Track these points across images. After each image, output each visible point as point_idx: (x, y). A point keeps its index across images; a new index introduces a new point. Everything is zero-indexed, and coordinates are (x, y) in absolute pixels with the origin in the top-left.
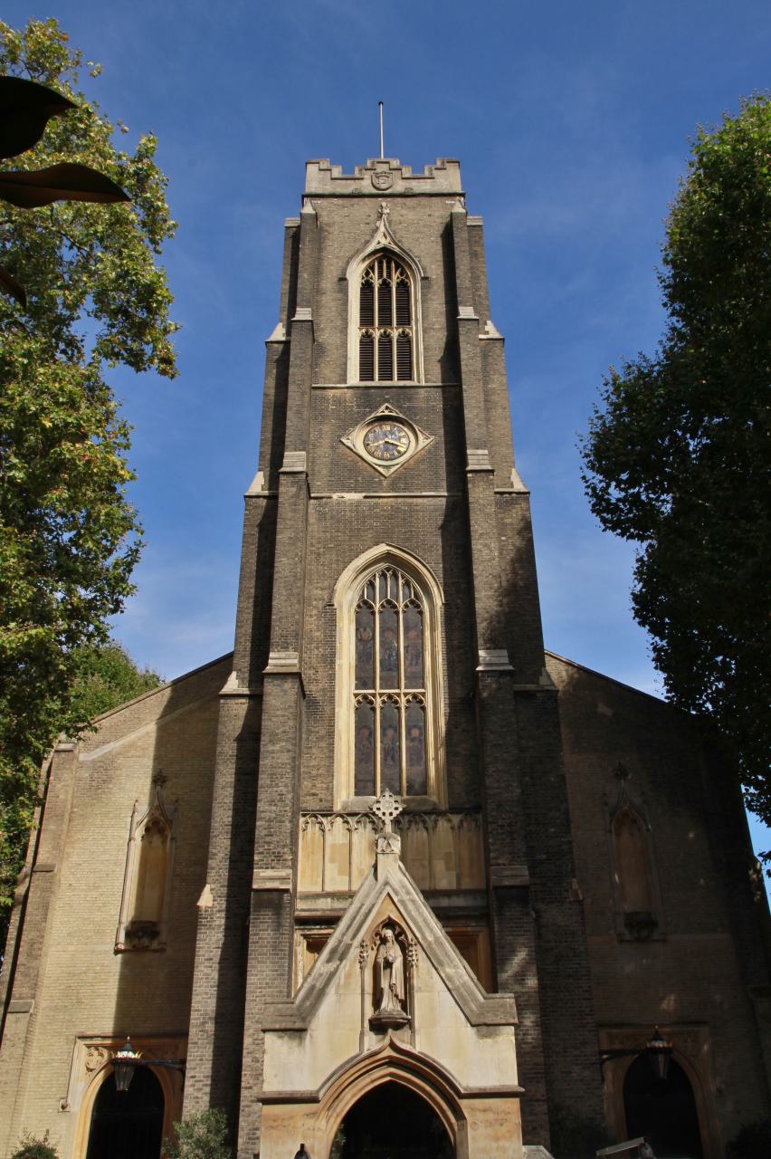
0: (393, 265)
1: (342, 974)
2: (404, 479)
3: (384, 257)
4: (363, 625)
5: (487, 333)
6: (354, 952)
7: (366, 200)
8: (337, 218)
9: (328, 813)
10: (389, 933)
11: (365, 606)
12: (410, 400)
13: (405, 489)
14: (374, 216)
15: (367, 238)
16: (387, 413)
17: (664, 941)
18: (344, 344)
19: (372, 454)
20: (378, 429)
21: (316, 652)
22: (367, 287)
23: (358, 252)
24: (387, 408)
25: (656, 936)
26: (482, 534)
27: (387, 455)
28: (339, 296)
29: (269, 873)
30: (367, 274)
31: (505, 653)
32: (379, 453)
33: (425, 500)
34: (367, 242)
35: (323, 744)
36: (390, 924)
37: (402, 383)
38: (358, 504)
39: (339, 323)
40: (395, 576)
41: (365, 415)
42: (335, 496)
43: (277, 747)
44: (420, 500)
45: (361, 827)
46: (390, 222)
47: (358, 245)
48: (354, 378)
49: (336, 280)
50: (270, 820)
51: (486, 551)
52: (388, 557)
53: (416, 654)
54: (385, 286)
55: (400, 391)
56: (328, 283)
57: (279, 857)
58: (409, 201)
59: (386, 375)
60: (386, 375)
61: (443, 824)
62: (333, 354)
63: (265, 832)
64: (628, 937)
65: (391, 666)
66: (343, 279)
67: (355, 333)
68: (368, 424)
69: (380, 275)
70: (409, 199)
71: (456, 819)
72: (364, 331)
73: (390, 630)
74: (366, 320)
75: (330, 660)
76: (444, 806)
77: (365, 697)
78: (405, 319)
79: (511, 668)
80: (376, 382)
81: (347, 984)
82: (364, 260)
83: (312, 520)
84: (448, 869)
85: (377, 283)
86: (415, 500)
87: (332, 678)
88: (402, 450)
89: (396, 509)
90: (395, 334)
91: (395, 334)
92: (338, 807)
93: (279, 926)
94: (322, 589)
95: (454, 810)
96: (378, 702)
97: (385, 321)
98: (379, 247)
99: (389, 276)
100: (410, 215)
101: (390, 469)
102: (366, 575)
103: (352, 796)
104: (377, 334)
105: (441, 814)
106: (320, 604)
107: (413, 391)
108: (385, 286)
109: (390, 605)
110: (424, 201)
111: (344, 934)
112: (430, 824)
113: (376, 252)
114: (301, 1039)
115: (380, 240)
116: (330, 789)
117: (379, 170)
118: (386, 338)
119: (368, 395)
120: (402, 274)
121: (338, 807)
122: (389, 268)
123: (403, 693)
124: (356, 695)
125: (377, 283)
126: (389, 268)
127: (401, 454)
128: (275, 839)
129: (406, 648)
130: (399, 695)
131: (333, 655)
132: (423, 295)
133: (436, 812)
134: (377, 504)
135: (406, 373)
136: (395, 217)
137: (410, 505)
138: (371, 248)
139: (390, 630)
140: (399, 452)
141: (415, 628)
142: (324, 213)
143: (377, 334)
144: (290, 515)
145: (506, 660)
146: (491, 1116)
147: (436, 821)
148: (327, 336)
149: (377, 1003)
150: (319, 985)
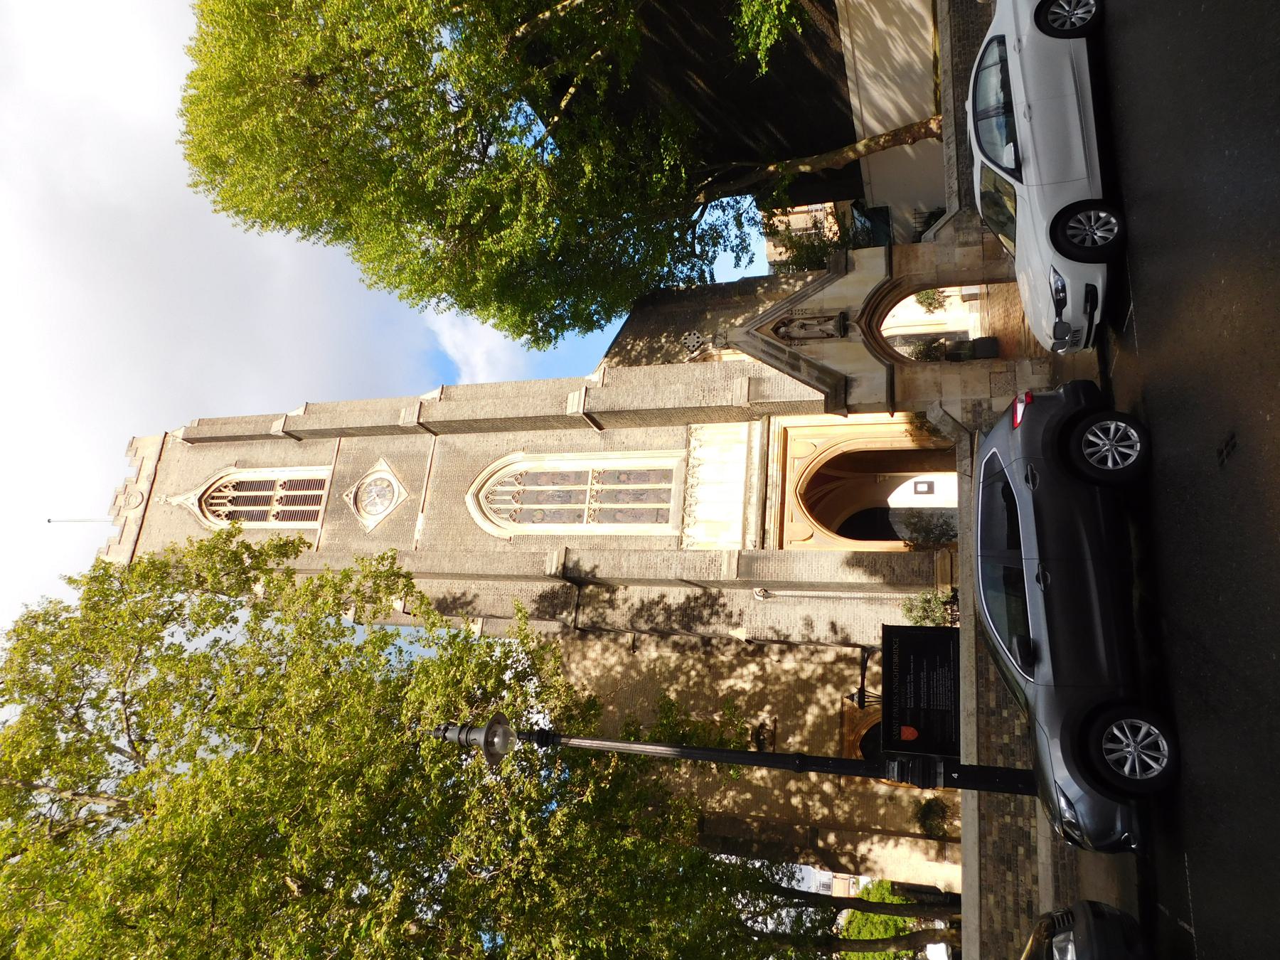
1: (809, 357)
2: (414, 484)
4: (529, 517)
6: (794, 349)
9: (680, 541)
10: (783, 330)
11: (515, 517)
12: (344, 477)
13: (422, 481)
14: (167, 508)
15: (185, 513)
16: (352, 496)
29: (724, 568)
31: (570, 396)
32: (387, 503)
36: (776, 330)
37: (327, 485)
38: (428, 518)
42: (417, 536)
43: (625, 564)
45: (693, 515)
47: (191, 521)
50: (683, 569)
51: (487, 409)
52: (477, 496)
53: (563, 477)
54: (234, 501)
55: (334, 485)
57: (713, 561)
59: (317, 500)
60: (317, 500)
63: (692, 573)
65: (567, 497)
67: (272, 524)
69: (224, 504)
73: (537, 498)
76: (683, 453)
81: (816, 353)
85: (230, 508)
88: (386, 484)
93: (766, 558)
101: (401, 493)
103: (670, 524)
105: (689, 455)
107: (337, 476)
108: (234, 501)
111: (782, 361)
112: (696, 462)
113: (200, 506)
114: (853, 380)
118: (280, 501)
119: (333, 511)
121: (677, 533)
122: (218, 498)
123: (592, 487)
125: (230, 508)
126: (218, 498)
127: (390, 485)
128: (698, 565)
129: (554, 484)
132: (252, 466)
134: (431, 504)
135: (319, 484)
136: (171, 490)
139: (537, 498)
143: (276, 508)
144: (429, 562)
145: (577, 393)
146: (904, 261)
149: (830, 336)
150: (816, 373)
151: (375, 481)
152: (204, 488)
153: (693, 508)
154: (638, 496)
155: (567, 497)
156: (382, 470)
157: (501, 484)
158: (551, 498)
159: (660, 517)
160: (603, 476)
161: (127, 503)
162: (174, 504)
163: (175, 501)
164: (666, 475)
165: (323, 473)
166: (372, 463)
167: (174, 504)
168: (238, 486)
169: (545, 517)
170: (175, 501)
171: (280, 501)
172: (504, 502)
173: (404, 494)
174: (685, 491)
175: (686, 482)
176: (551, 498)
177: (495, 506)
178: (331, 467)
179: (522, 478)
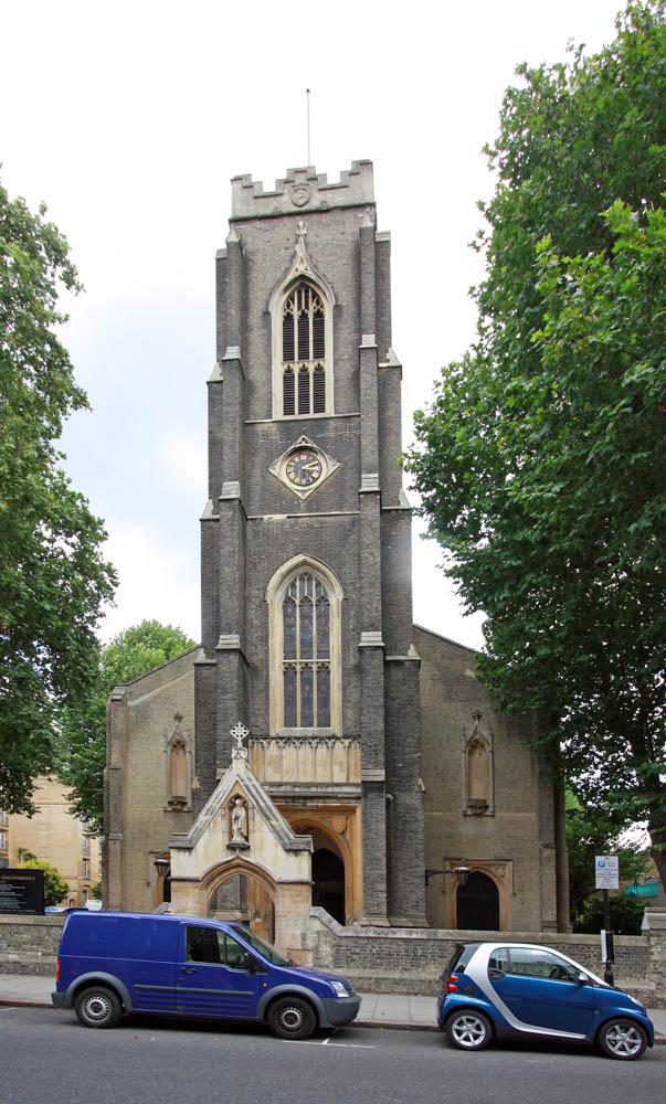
0: (310, 294)
2: (314, 502)
3: (302, 285)
5: (388, 361)
7: (286, 220)
8: (260, 246)
11: (288, 601)
13: (317, 510)
14: (292, 240)
15: (287, 265)
16: (304, 444)
17: (493, 816)
18: (269, 380)
19: (292, 481)
20: (297, 459)
21: (255, 634)
22: (288, 318)
23: (280, 281)
24: (304, 439)
25: (488, 813)
26: (368, 545)
27: (304, 482)
28: (264, 331)
30: (288, 306)
32: (297, 480)
33: (332, 518)
34: (287, 270)
35: (262, 695)
38: (282, 523)
39: (264, 359)
40: (310, 579)
41: (288, 446)
42: (266, 517)
44: (328, 518)
46: (306, 245)
47: (279, 275)
48: (278, 413)
49: (261, 314)
52: (304, 563)
53: (324, 635)
54: (304, 316)
55: (314, 423)
56: (255, 319)
58: (325, 218)
59: (304, 410)
60: (304, 410)
61: (338, 744)
62: (260, 391)
64: (469, 813)
65: (306, 644)
66: (267, 314)
68: (290, 455)
70: (324, 215)
71: (347, 742)
72: (286, 366)
74: (288, 356)
75: (265, 639)
77: (290, 664)
78: (320, 353)
79: (383, 644)
80: (297, 416)
82: (286, 290)
83: (249, 538)
84: (341, 771)
85: (296, 314)
86: (324, 518)
87: (267, 652)
88: (315, 475)
89: (310, 527)
90: (311, 367)
91: (311, 367)
92: (273, 734)
94: (259, 590)
95: (346, 737)
96: (298, 668)
97: (304, 356)
98: (297, 274)
99: (307, 307)
100: (325, 236)
101: (302, 493)
102: (287, 582)
104: (296, 368)
105: (338, 738)
106: (257, 601)
107: (324, 423)
108: (304, 316)
109: (305, 600)
110: (338, 216)
113: (295, 280)
115: (301, 268)
116: (267, 723)
117: (297, 182)
118: (304, 370)
120: (318, 303)
121: (273, 734)
122: (307, 297)
123: (314, 661)
124: (284, 663)
125: (296, 314)
126: (307, 297)
127: (315, 480)
130: (312, 663)
131: (267, 636)
132: (335, 325)
133: (334, 737)
135: (320, 407)
136: (311, 239)
137: (321, 522)
138: (290, 277)
139: (306, 617)
140: (313, 478)
141: (324, 617)
142: (249, 240)
143: (296, 368)
147: (334, 743)
148: (256, 374)
151: (319, 464)
152: (313, 277)
153: (292, 746)
154: (307, 701)
155: (306, 644)
156: (326, 467)
157: (318, 584)
158: (305, 630)
159: (289, 721)
160: (324, 669)
161: (296, 189)
162: (297, 248)
163: (300, 250)
164: (325, 722)
165: (330, 410)
166: (336, 456)
167: (297, 248)
168: (319, 315)
169: (288, 627)
170: (300, 250)
171: (304, 370)
172: (302, 591)
173: (303, 496)
174: (305, 738)
175: (314, 738)
176: (305, 630)
177: (298, 584)
178: (333, 415)
179: (323, 600)
